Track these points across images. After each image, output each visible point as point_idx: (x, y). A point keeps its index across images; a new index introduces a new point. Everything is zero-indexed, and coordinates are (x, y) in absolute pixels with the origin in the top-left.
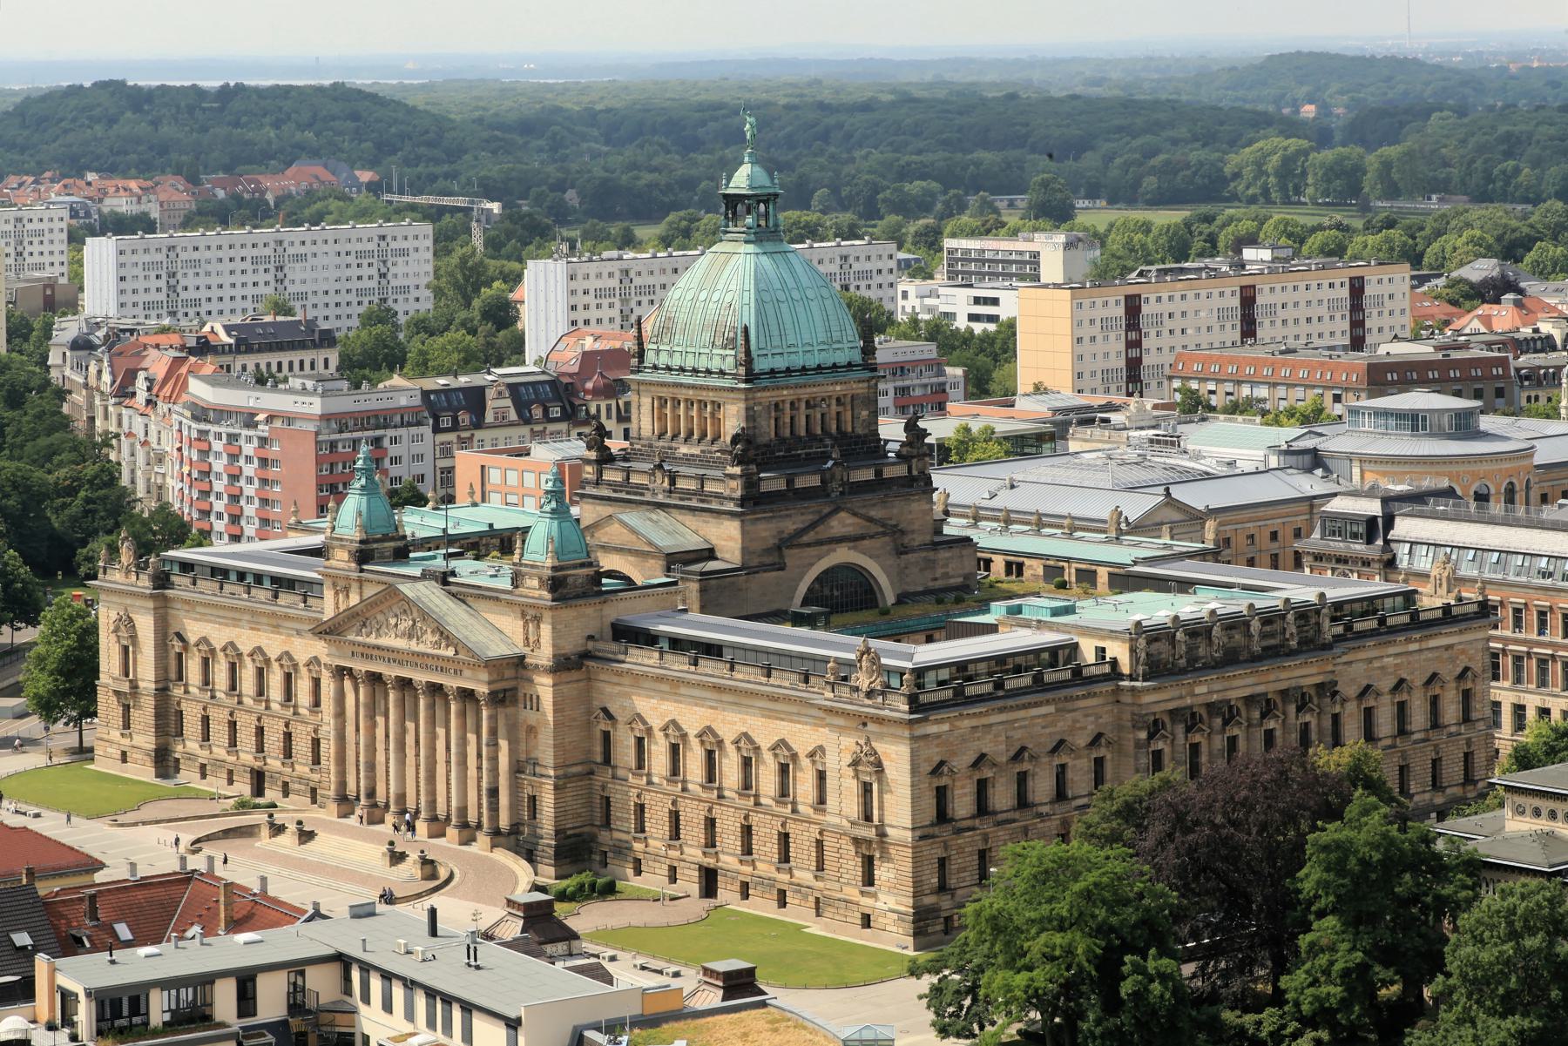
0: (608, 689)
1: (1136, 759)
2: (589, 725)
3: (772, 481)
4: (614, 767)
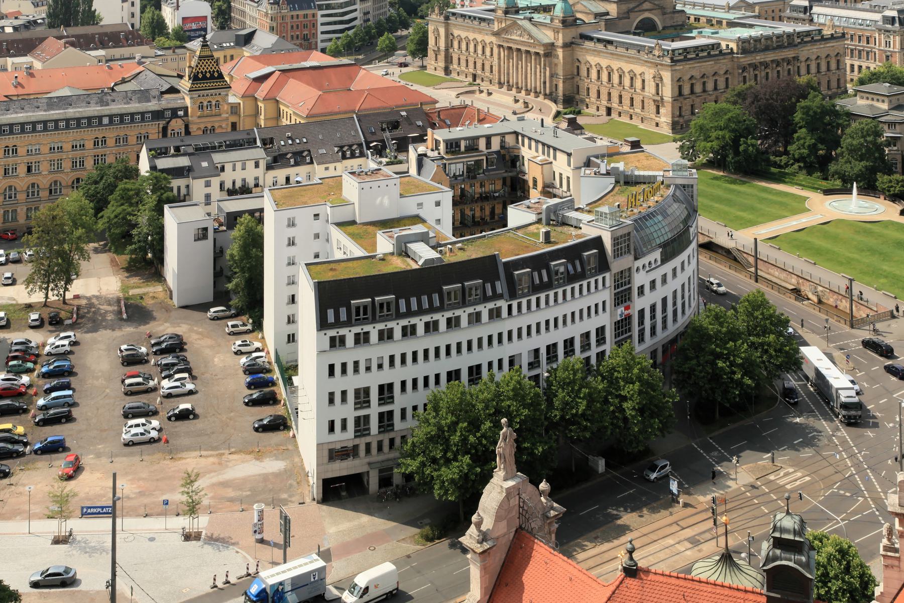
2: (573, 64)
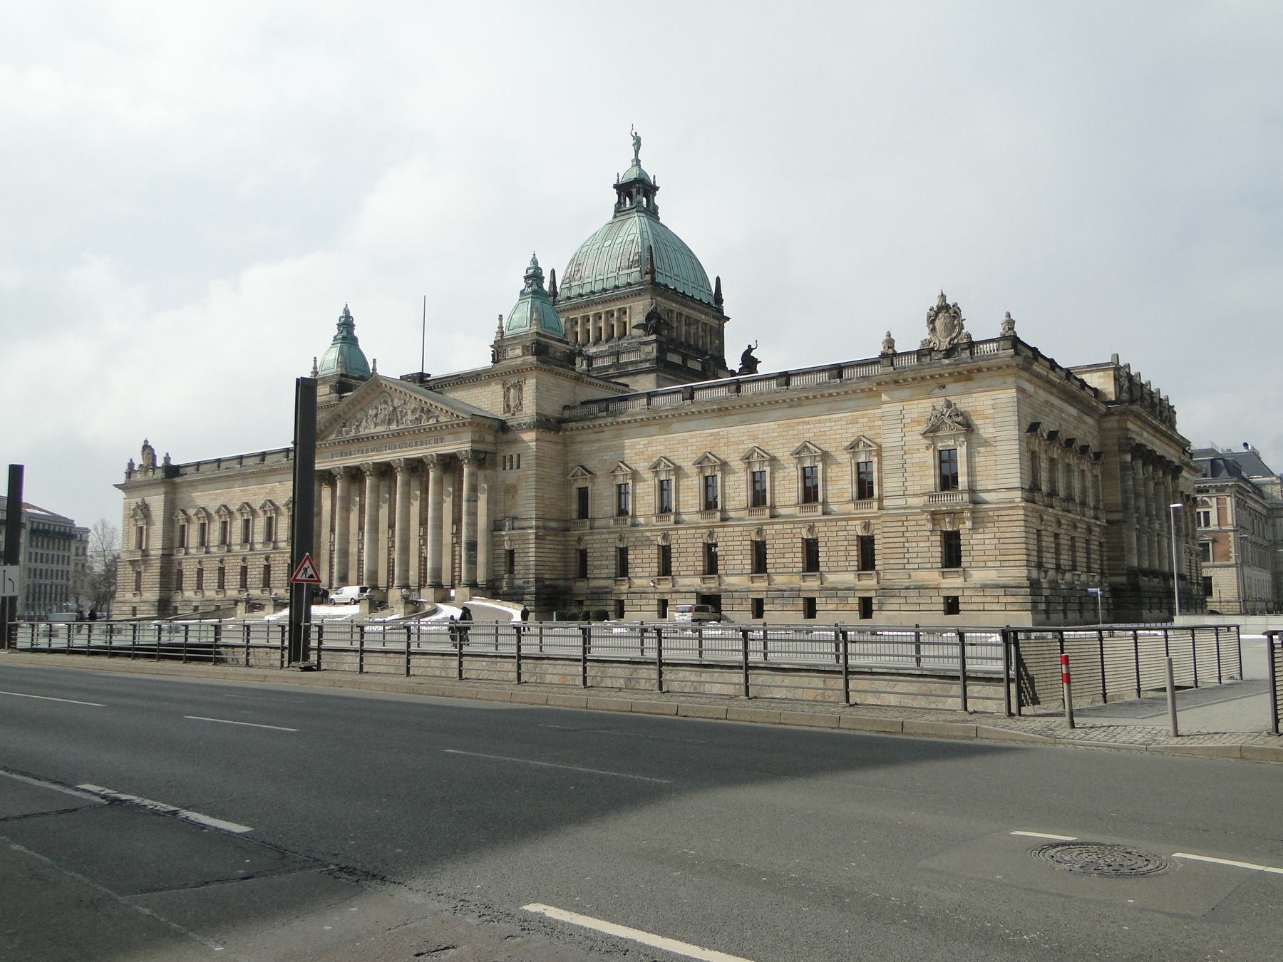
0: (586, 449)
1: (1123, 481)
2: (566, 484)
3: (674, 358)
4: (593, 519)
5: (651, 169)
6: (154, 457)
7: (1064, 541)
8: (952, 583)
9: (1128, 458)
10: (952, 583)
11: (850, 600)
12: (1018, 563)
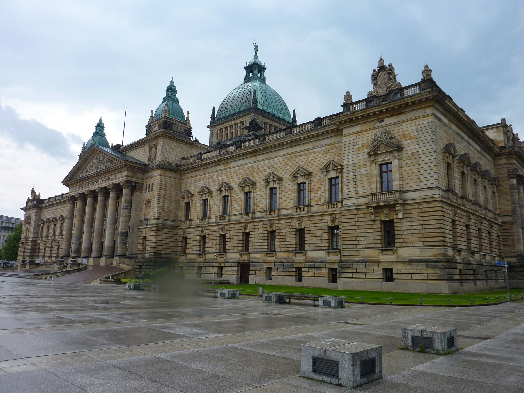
0: (190, 180)
1: (512, 196)
4: (191, 220)
5: (262, 60)
6: (35, 195)
7: (474, 231)
8: (388, 258)
9: (515, 182)
10: (388, 258)
11: (323, 270)
12: (437, 244)
